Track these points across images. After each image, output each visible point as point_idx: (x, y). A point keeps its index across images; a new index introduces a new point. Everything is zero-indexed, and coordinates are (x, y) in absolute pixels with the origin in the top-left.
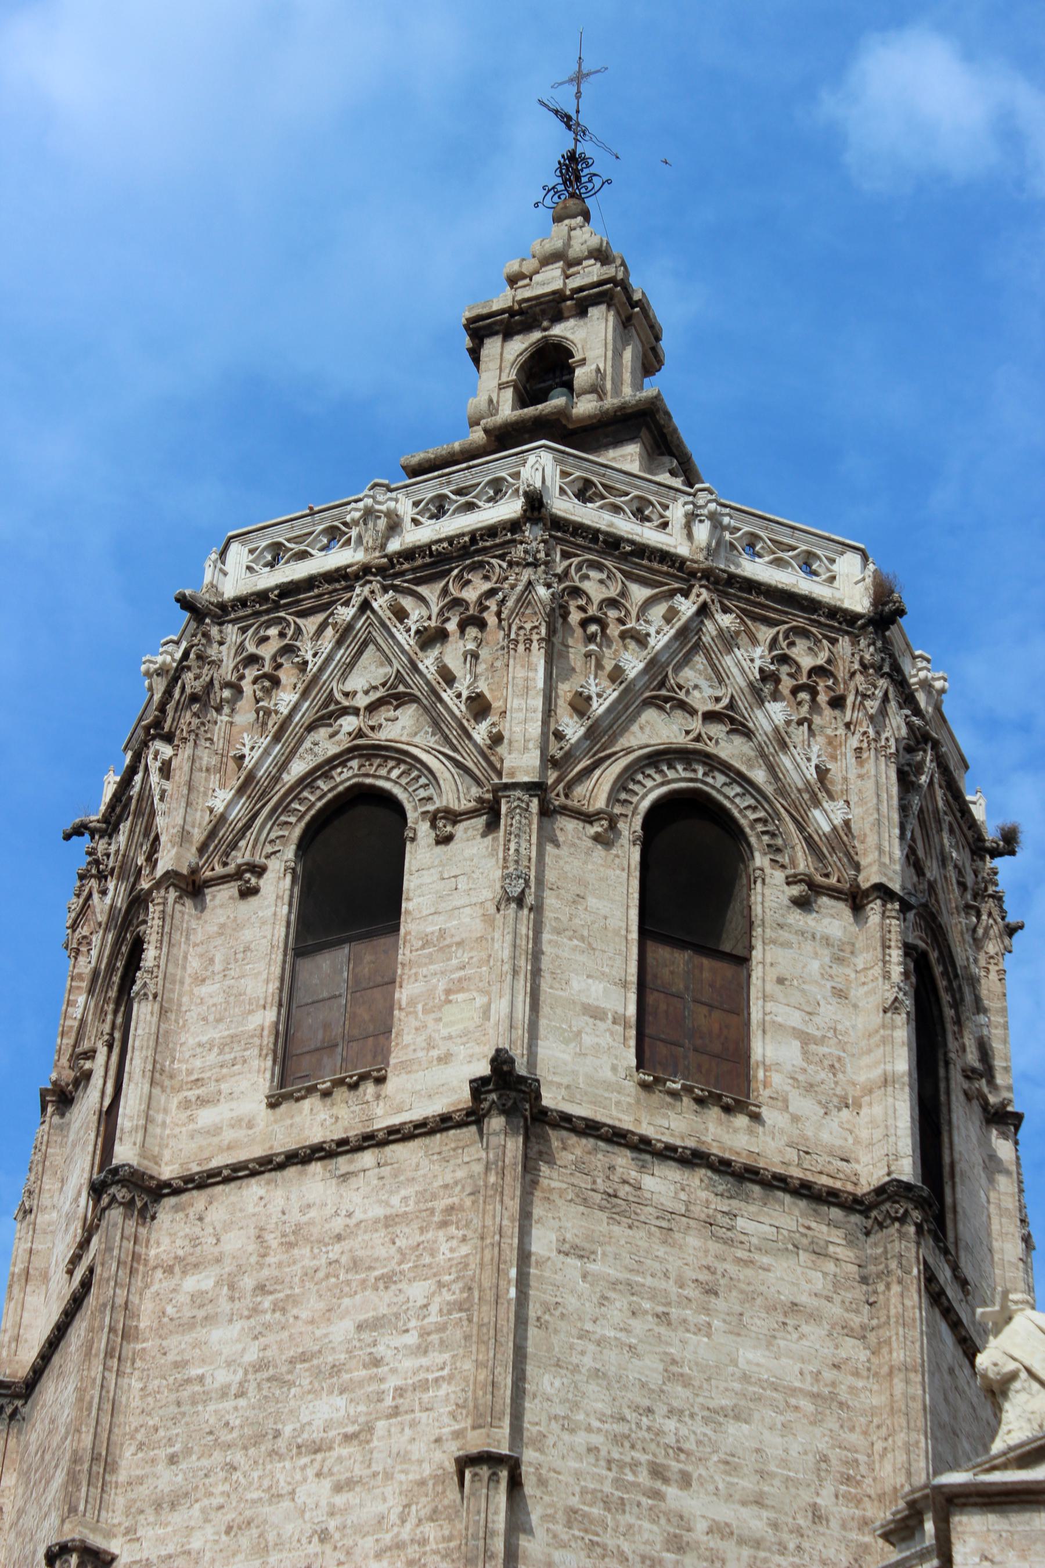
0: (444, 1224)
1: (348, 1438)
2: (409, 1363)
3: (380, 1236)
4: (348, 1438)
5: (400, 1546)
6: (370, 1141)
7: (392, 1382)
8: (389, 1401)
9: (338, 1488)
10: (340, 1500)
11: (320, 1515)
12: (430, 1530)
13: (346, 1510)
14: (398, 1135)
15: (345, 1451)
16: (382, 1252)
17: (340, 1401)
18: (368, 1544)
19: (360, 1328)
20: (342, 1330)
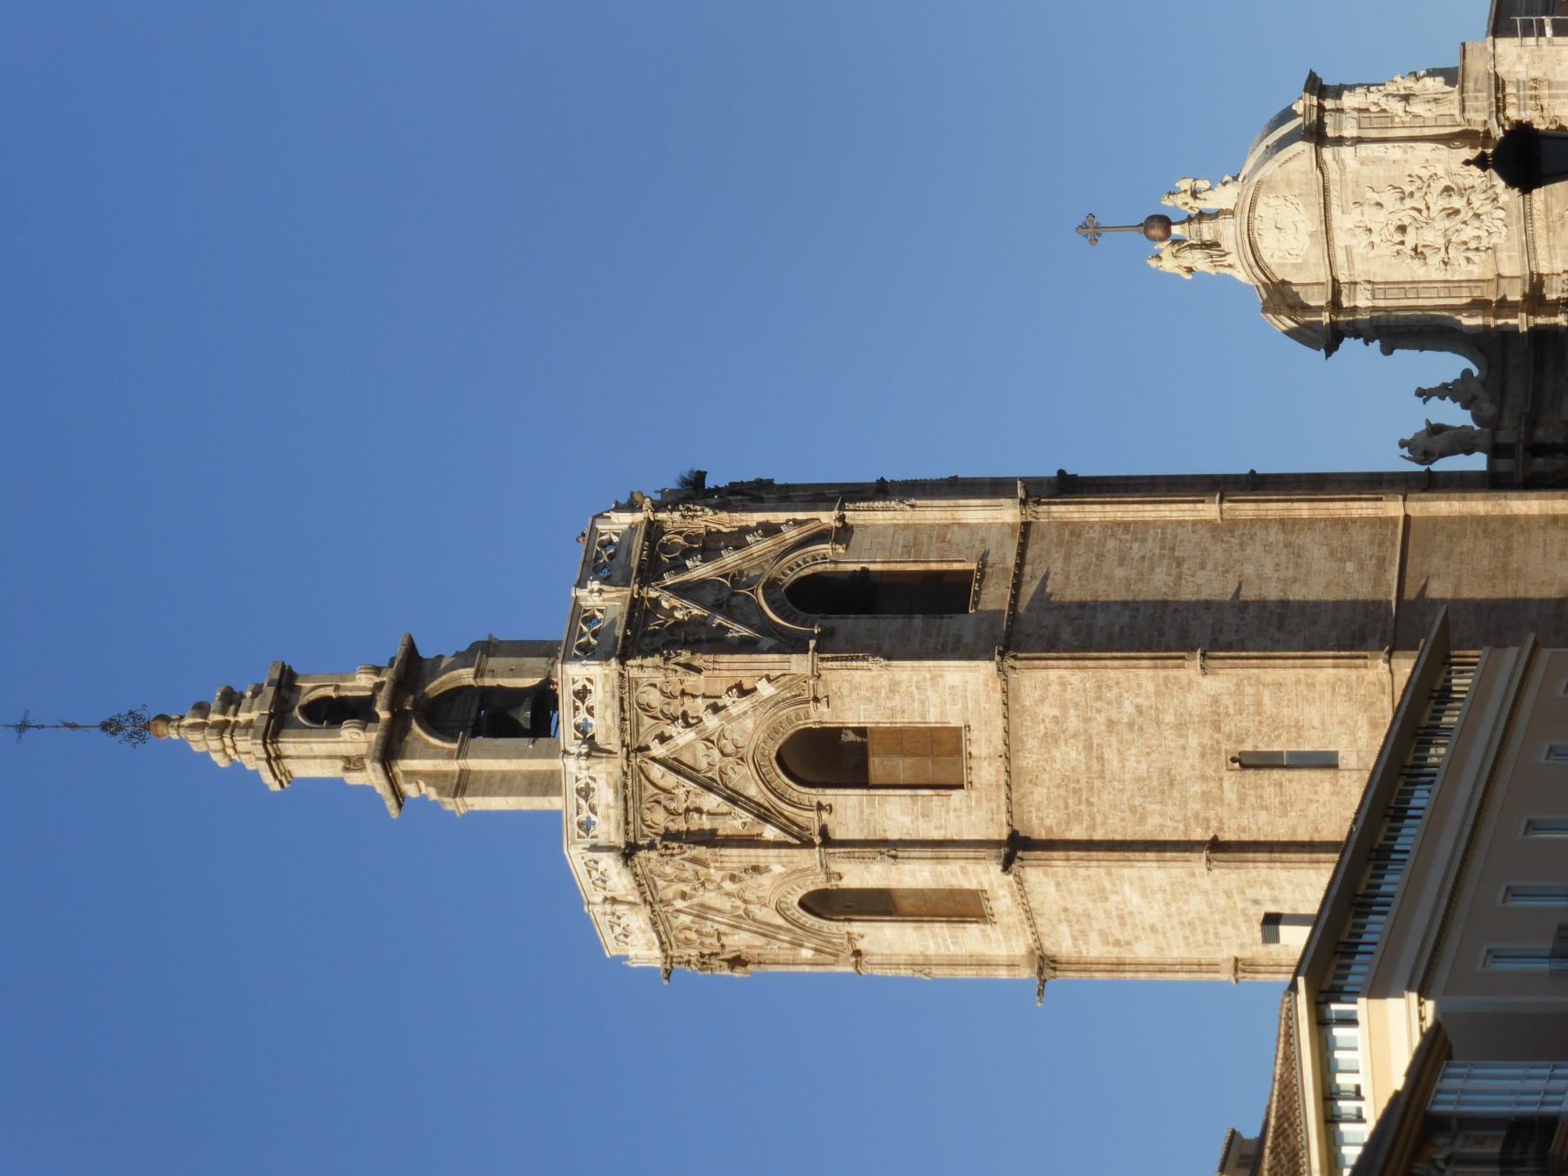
0: (1079, 536)
1: (1179, 565)
2: (1149, 545)
3: (1075, 561)
4: (1179, 565)
5: (1241, 544)
6: (1020, 565)
7: (1157, 552)
8: (1166, 552)
9: (1203, 566)
10: (1209, 566)
11: (1214, 575)
12: (1237, 533)
13: (1216, 564)
14: (1021, 554)
15: (1185, 568)
16: (1084, 559)
17: (1158, 570)
18: (1236, 555)
19: (1121, 565)
20: (1119, 573)
